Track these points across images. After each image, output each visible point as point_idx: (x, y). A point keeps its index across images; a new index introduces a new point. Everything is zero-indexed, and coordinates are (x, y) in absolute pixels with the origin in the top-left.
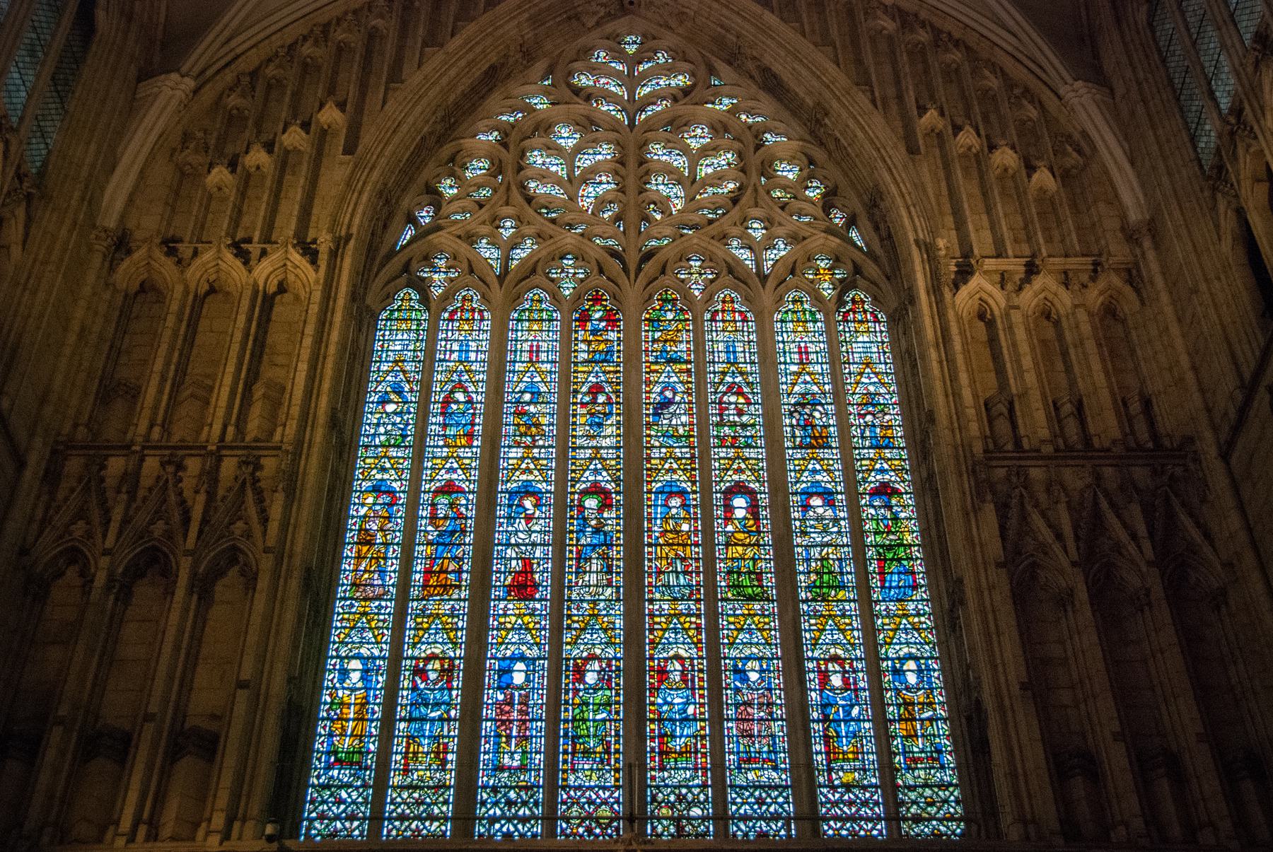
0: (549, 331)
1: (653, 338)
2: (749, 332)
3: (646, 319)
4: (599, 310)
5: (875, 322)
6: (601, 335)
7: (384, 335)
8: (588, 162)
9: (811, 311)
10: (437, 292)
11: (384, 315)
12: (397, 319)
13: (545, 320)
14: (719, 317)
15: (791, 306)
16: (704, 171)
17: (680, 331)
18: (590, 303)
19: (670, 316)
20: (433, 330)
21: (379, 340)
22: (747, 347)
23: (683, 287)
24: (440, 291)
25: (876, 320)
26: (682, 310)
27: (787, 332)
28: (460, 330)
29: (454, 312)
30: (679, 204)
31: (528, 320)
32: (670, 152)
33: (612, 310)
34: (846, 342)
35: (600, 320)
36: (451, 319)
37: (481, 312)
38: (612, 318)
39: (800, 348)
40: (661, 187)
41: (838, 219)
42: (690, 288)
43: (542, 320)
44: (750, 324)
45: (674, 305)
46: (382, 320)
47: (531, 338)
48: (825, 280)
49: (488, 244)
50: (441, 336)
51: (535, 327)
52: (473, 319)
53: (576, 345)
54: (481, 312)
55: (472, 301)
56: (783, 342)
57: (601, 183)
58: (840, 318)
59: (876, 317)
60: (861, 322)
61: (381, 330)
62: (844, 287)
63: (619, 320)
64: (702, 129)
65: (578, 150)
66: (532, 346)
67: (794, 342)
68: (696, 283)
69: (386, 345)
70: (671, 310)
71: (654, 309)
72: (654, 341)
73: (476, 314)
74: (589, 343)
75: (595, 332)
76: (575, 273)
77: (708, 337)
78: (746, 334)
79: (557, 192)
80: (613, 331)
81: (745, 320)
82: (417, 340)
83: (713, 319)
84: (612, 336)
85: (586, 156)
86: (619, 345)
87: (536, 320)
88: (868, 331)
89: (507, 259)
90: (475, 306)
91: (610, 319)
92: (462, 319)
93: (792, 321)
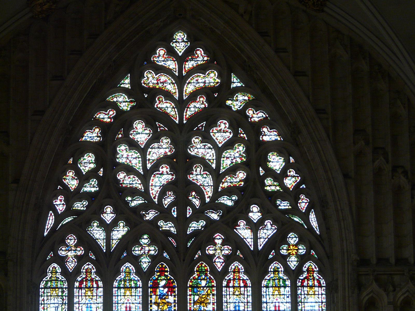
0: (135, 296)
1: (194, 300)
2: (247, 295)
3: (191, 286)
4: (164, 279)
5: (319, 287)
6: (165, 299)
7: (43, 300)
8: (154, 155)
9: (283, 279)
10: (71, 266)
11: (42, 285)
12: (50, 288)
13: (133, 288)
14: (231, 285)
15: (272, 275)
16: (226, 163)
17: (209, 295)
18: (158, 274)
19: (203, 283)
20: (71, 296)
21: (42, 304)
22: (246, 306)
23: (210, 259)
24: (73, 265)
25: (320, 286)
26: (210, 278)
27: (269, 295)
28: (86, 296)
29: (81, 282)
30: (209, 192)
31: (124, 288)
32: (205, 146)
33: (171, 279)
34: (301, 302)
35: (164, 287)
36: (80, 288)
37: (97, 282)
38: (171, 285)
39: (275, 307)
40: (199, 177)
41: (303, 204)
42: (215, 262)
43: (132, 288)
44: (248, 288)
45: (206, 275)
46: (42, 288)
47: (126, 301)
48: (293, 254)
49: (98, 227)
50: (76, 300)
51: (128, 293)
52: (93, 287)
53: (151, 306)
54: (97, 282)
55: (91, 272)
56: (266, 303)
57: (162, 174)
58: (300, 284)
59: (319, 282)
60: (311, 287)
61: (42, 296)
62: (302, 259)
63: (175, 287)
64: (225, 124)
65: (149, 144)
66: (126, 307)
67: (272, 303)
68: (219, 257)
69: (46, 308)
70: (204, 279)
71: (194, 278)
72: (195, 303)
73: (94, 283)
74: (157, 304)
75: (162, 297)
76: (149, 250)
77: (224, 299)
78: (246, 296)
79: (137, 184)
80: (171, 295)
81: (246, 286)
82: (63, 303)
83: (228, 286)
84: (171, 299)
85: (153, 150)
86: (175, 306)
87: (128, 288)
88: (314, 294)
89: (108, 239)
90: (93, 277)
91: (168, 286)
92: (86, 287)
93: (272, 287)
